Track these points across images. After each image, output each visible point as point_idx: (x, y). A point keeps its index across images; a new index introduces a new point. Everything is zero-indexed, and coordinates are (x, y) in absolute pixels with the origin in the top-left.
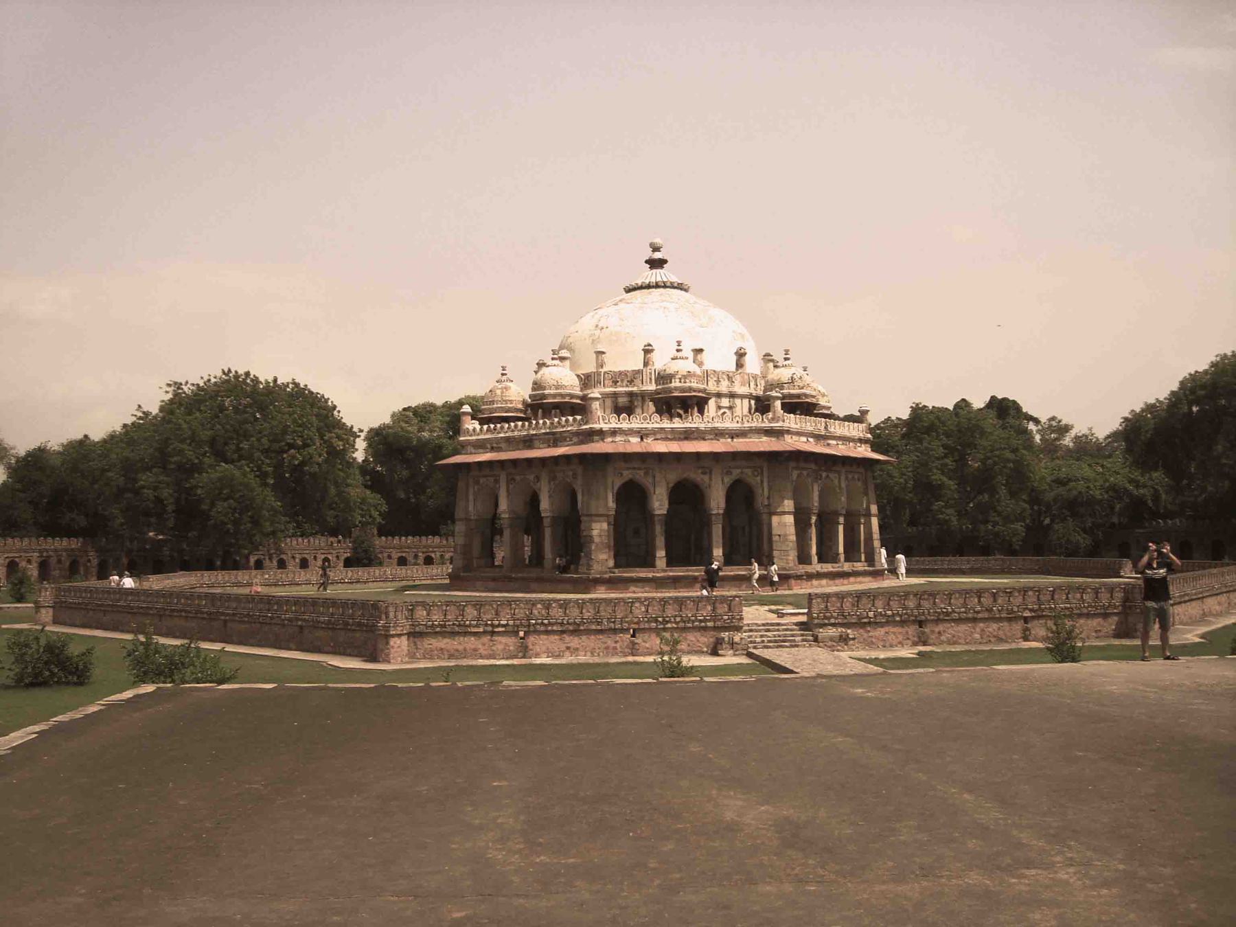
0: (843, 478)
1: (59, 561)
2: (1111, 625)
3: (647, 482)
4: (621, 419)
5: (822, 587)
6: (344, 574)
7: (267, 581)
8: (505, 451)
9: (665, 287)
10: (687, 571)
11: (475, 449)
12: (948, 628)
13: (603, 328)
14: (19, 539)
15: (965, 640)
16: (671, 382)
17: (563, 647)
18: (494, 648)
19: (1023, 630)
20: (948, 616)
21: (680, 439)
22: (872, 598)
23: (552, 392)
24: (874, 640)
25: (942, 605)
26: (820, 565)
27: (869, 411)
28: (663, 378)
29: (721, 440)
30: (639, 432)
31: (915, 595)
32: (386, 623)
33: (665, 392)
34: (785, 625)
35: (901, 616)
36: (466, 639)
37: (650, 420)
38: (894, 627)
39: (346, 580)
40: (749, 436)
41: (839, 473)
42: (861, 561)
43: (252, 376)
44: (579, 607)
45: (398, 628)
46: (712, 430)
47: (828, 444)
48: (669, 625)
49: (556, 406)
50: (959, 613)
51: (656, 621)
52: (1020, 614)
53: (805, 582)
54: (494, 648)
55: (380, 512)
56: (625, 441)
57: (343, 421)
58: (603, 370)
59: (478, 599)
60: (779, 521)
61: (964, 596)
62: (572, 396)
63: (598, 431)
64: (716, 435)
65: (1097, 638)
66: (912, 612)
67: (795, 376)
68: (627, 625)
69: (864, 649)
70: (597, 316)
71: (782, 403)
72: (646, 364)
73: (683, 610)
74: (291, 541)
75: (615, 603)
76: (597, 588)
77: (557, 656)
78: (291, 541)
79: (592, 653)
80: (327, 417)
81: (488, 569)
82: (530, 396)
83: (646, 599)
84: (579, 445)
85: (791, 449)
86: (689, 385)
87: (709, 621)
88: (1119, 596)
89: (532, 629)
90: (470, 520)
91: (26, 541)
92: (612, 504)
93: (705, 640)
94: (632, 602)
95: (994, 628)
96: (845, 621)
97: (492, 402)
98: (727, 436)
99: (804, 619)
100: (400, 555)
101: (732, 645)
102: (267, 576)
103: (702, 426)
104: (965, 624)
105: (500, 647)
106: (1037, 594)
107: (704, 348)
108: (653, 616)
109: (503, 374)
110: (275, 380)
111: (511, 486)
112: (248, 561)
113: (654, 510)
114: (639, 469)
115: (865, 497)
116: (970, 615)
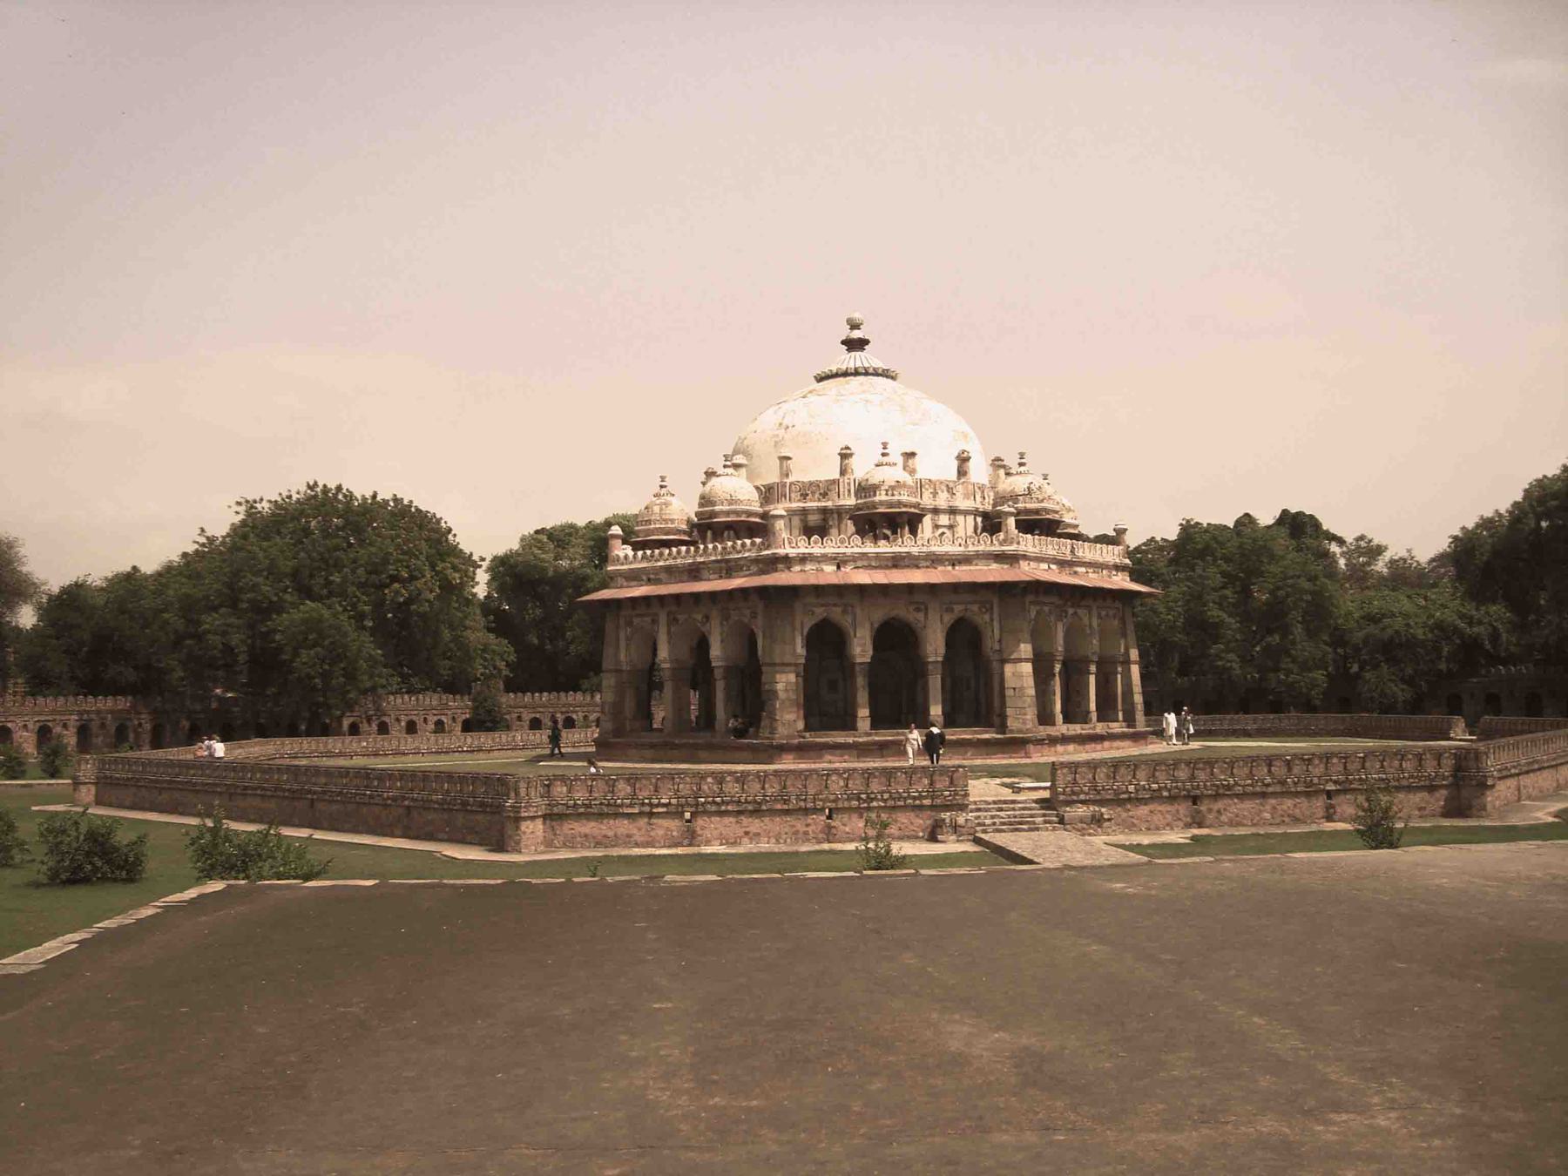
0: (1095, 612)
1: (103, 726)
2: (1438, 800)
3: (846, 622)
4: (812, 542)
5: (1069, 754)
6: (463, 740)
7: (364, 750)
8: (666, 583)
9: (866, 373)
10: (898, 734)
11: (627, 581)
12: (1230, 805)
13: (788, 427)
16: (875, 495)
17: (740, 832)
18: (652, 834)
21: (887, 567)
22: (1133, 767)
23: (726, 508)
25: (1222, 777)
26: (1065, 726)
27: (1126, 530)
28: (865, 489)
29: (940, 568)
30: (835, 559)
31: (1188, 764)
32: (516, 802)
33: (868, 508)
34: (1023, 803)
35: (1169, 791)
36: (617, 821)
38: (1160, 805)
39: (465, 749)
40: (974, 563)
41: (1089, 608)
42: (1117, 721)
43: (344, 491)
44: (760, 781)
45: (531, 809)
47: (1076, 573)
48: (875, 804)
49: (729, 526)
50: (1244, 786)
51: (859, 799)
53: (1048, 749)
54: (652, 834)
55: (507, 662)
56: (817, 570)
57: (460, 546)
59: (631, 771)
61: (1250, 765)
62: (750, 514)
63: (783, 557)
64: (933, 561)
65: (1420, 817)
66: (1184, 786)
68: (821, 803)
69: (1120, 833)
70: (781, 413)
71: (1016, 521)
72: (843, 472)
73: (892, 784)
74: (395, 699)
75: (805, 775)
76: (784, 756)
77: (732, 844)
78: (395, 699)
79: (777, 840)
80: (439, 542)
81: (643, 734)
82: (697, 514)
83: (846, 770)
84: (759, 575)
85: (1028, 579)
87: (925, 797)
89: (701, 809)
91: (61, 700)
92: (800, 650)
93: (921, 822)
94: (828, 775)
95: (1289, 805)
96: (1098, 797)
97: (649, 522)
98: (947, 563)
99: (1046, 794)
100: (534, 715)
101: (955, 828)
102: (365, 744)
103: (915, 550)
104: (1250, 800)
105: (661, 832)
106: (1344, 761)
107: (916, 451)
108: (855, 792)
109: (662, 487)
110: (374, 496)
111: (672, 629)
112: (340, 725)
113: (854, 657)
114: (835, 605)
116: (1258, 789)
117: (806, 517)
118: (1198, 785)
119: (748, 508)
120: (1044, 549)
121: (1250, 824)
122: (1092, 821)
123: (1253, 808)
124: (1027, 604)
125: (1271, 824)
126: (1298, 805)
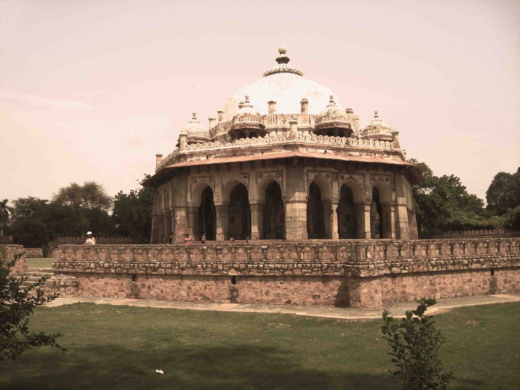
2: (333, 289)
3: (211, 185)
9: (279, 72)
15: (173, 296)
19: (230, 291)
20: (155, 271)
21: (230, 156)
24: (96, 289)
29: (255, 155)
35: (115, 269)
37: (213, 145)
38: (112, 279)
40: (273, 151)
46: (249, 148)
47: (350, 155)
50: (165, 269)
52: (225, 272)
58: (220, 123)
60: (291, 208)
63: (182, 155)
64: (252, 151)
65: (314, 304)
67: (330, 112)
86: (244, 121)
88: (346, 256)
90: (158, 215)
95: (201, 286)
96: (74, 270)
98: (259, 152)
103: (243, 147)
113: (214, 203)
114: (206, 177)
115: (394, 192)
116: (176, 272)
117: (226, 139)
118: (134, 265)
120: (321, 142)
121: (171, 299)
122: (54, 286)
123: (174, 286)
124: (305, 171)
125: (185, 301)
126: (208, 287)
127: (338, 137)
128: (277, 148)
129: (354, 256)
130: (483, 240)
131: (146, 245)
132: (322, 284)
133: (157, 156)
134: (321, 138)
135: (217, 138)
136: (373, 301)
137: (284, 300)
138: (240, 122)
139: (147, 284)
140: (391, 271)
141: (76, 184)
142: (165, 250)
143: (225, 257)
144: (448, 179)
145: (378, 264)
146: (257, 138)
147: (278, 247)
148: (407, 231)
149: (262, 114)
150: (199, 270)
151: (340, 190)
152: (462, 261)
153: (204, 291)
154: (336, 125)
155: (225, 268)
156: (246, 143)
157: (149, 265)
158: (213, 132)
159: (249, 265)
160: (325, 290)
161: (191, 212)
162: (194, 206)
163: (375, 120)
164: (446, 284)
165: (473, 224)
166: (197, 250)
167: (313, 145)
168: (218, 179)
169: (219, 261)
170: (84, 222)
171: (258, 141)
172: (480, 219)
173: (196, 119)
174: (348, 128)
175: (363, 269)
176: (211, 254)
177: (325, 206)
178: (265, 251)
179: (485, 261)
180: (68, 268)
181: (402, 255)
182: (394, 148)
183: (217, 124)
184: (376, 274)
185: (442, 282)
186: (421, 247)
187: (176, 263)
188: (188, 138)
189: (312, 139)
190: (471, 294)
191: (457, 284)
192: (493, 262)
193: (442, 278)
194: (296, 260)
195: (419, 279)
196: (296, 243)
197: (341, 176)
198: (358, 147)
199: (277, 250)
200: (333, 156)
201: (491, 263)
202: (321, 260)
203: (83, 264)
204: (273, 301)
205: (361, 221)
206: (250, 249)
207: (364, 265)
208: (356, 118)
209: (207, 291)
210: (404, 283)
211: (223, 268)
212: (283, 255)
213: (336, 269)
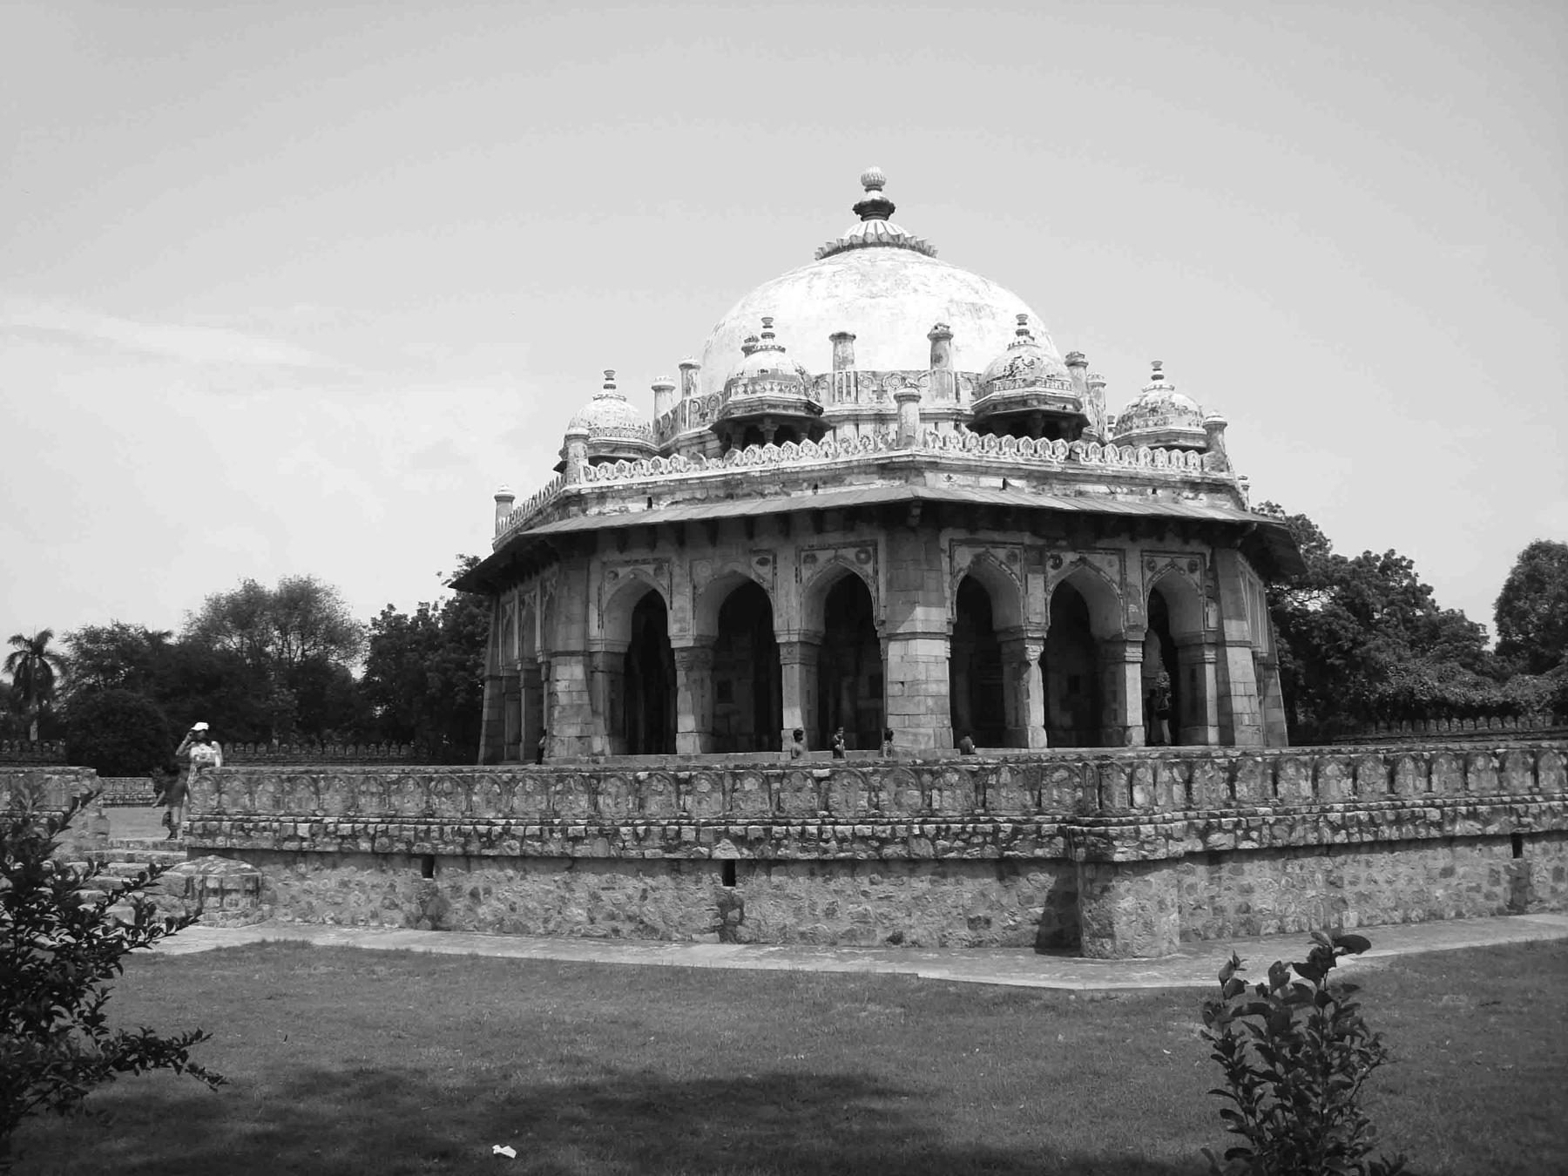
2: (1030, 900)
3: (661, 585)
9: (864, 245)
14: (340, 746)
15: (546, 921)
19: (720, 905)
20: (491, 845)
21: (718, 499)
24: (314, 903)
29: (794, 494)
35: (373, 839)
38: (363, 869)
40: (846, 482)
46: (774, 474)
47: (1080, 493)
50: (523, 838)
52: (704, 850)
58: (688, 398)
63: (575, 496)
65: (972, 945)
67: (1019, 362)
86: (759, 395)
95: (630, 891)
96: (247, 845)
98: (805, 485)
103: (755, 470)
113: (669, 641)
114: (645, 562)
115: (1214, 605)
116: (553, 848)
119: (619, 439)
120: (993, 454)
121: (541, 931)
122: (186, 891)
123: (551, 892)
124: (945, 544)
125: (584, 936)
126: (651, 895)
127: (1044, 438)
128: (859, 473)
129: (1094, 799)
130: (1488, 749)
131: (466, 768)
132: (998, 883)
133: (499, 499)
134: (993, 444)
135: (678, 446)
136: (1153, 935)
137: (881, 935)
138: (746, 396)
139: (468, 887)
140: (1205, 842)
141: (256, 587)
142: (521, 784)
143: (705, 802)
144: (1378, 564)
145: (1165, 821)
146: (798, 444)
147: (864, 774)
148: (1254, 721)
149: (813, 372)
150: (624, 842)
151: (1049, 598)
152: (1425, 812)
153: (640, 907)
154: (1035, 403)
155: (704, 838)
156: (765, 458)
157: (475, 829)
158: (666, 427)
159: (775, 828)
160: (1004, 901)
161: (600, 669)
162: (610, 649)
163: (1155, 388)
164: (1375, 882)
165: (1457, 702)
166: (619, 783)
167: (966, 463)
168: (681, 567)
169: (685, 814)
170: (282, 700)
171: (801, 454)
172: (1476, 685)
173: (613, 387)
174: (1074, 412)
175: (1120, 836)
176: (661, 793)
177: (1005, 650)
178: (824, 784)
179: (1494, 812)
180: (229, 836)
181: (1238, 795)
182: (1213, 472)
183: (677, 402)
184: (1161, 854)
185: (1363, 876)
186: (1298, 770)
187: (556, 821)
188: (592, 446)
189: (964, 447)
190: (1453, 914)
191: (1411, 880)
192: (1519, 816)
193: (1363, 864)
194: (918, 813)
195: (1294, 867)
196: (919, 761)
197: (1052, 557)
198: (1102, 468)
199: (859, 781)
200: (1028, 498)
201: (1514, 819)
202: (992, 812)
203: (275, 825)
204: (851, 936)
205: (1115, 693)
206: (780, 778)
207: (1124, 825)
208: (1097, 381)
209: (649, 907)
210: (1247, 880)
211: (697, 838)
212: (877, 796)
213: (1040, 838)
